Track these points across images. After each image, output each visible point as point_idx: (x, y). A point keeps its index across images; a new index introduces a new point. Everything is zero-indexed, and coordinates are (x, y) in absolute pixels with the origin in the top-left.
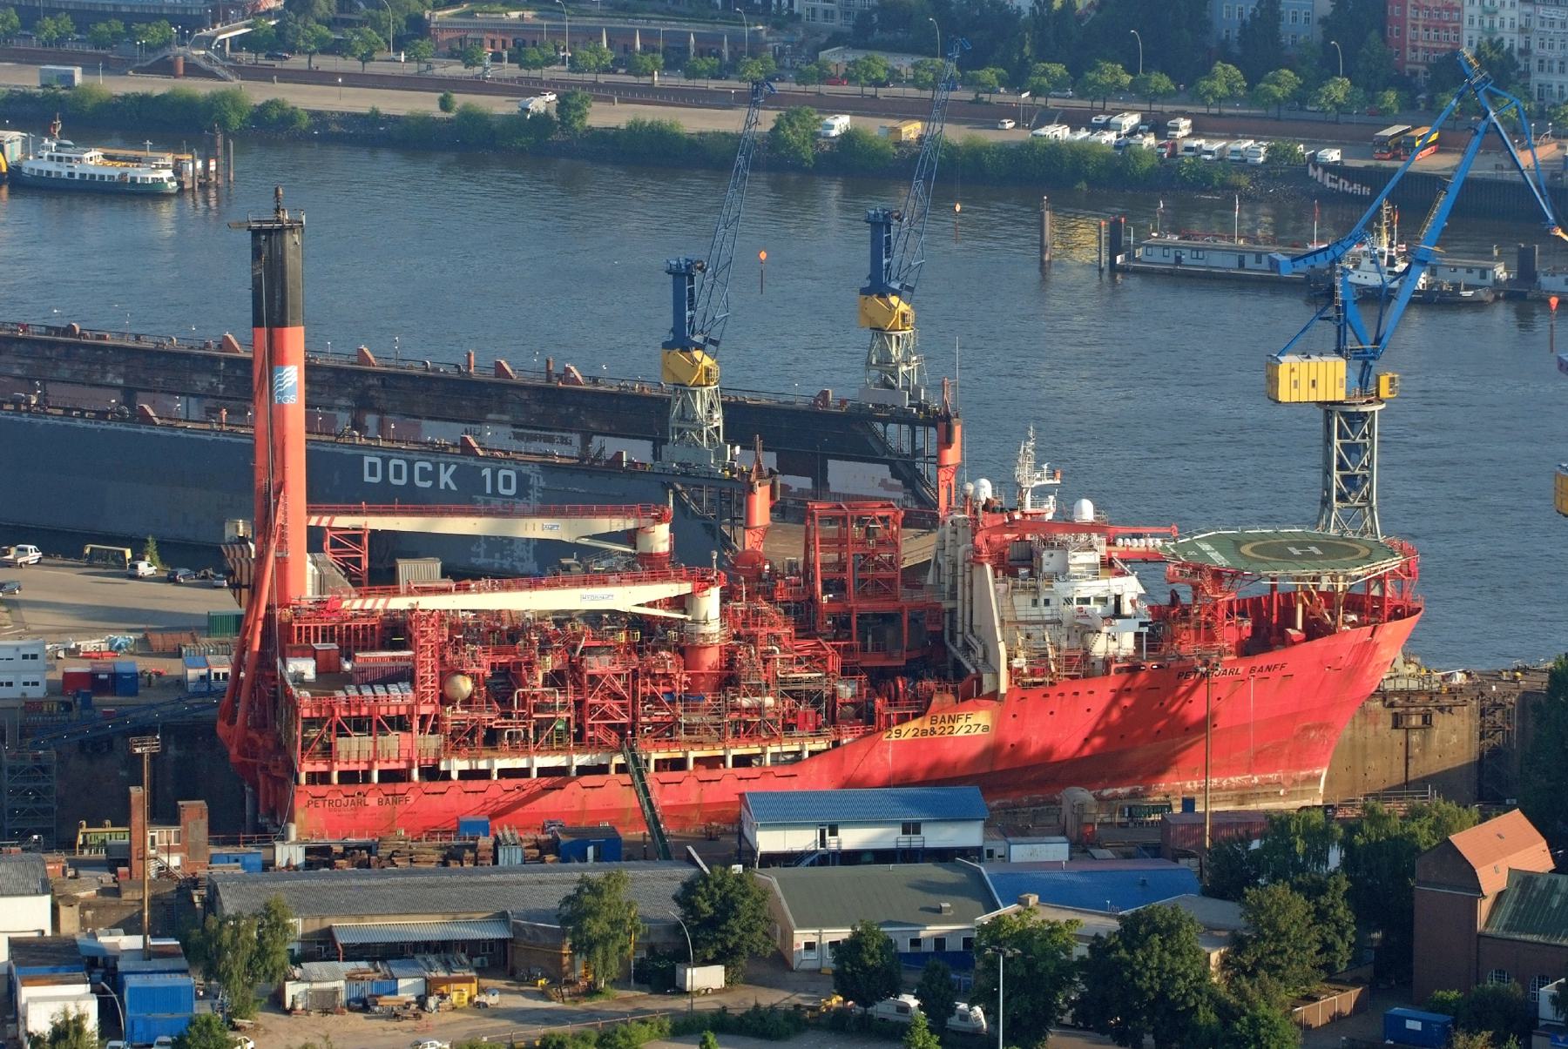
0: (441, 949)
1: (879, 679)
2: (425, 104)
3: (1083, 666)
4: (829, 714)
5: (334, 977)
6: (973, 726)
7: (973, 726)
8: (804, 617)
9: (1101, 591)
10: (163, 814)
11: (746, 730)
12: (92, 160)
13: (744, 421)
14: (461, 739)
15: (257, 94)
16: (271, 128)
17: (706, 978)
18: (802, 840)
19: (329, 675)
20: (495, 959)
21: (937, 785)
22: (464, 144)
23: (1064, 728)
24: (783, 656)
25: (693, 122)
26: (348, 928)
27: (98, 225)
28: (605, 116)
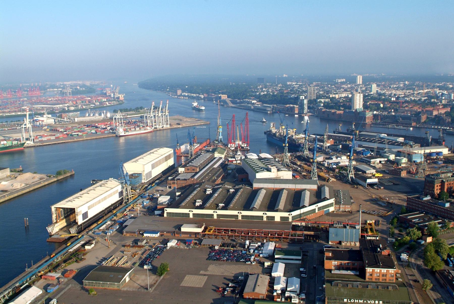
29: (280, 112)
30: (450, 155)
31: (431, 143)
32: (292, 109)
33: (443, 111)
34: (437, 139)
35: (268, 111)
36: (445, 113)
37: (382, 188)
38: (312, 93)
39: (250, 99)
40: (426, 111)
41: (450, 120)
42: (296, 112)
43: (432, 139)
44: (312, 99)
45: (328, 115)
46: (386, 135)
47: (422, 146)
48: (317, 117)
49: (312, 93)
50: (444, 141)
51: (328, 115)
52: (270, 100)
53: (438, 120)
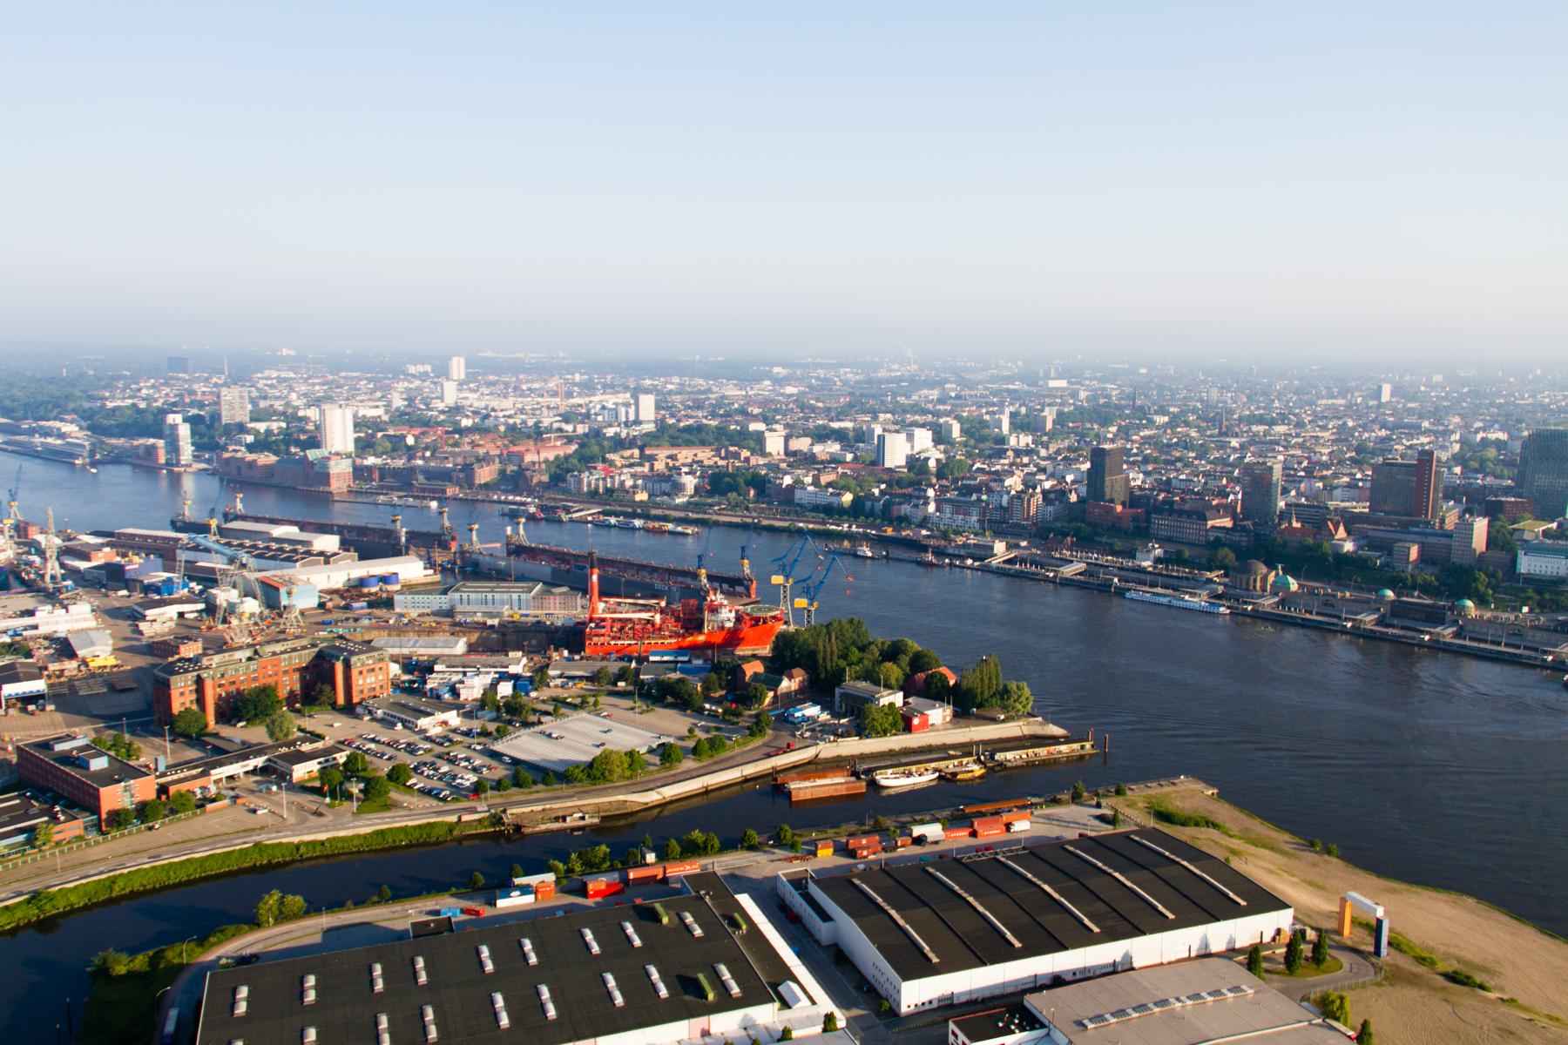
0: (581, 678)
1: (687, 630)
2: (738, 520)
3: (723, 628)
4: (677, 635)
5: (559, 681)
6: (701, 638)
7: (701, 638)
8: (678, 619)
9: (727, 616)
10: (556, 650)
11: (664, 637)
12: (679, 529)
13: (710, 578)
14: (614, 638)
15: (715, 517)
16: (717, 523)
17: (621, 684)
18: (657, 658)
19: (597, 626)
20: (588, 679)
21: (695, 649)
22: (744, 527)
23: (718, 639)
24: (671, 625)
25: (778, 524)
26: (568, 673)
27: (680, 540)
28: (765, 522)
29: (117, 459)
30: (429, 579)
31: (407, 549)
32: (151, 451)
33: (551, 456)
34: (439, 535)
35: (77, 457)
36: (557, 458)
37: (51, 707)
38: (237, 406)
39: (62, 420)
40: (510, 454)
41: (545, 478)
42: (162, 460)
43: (412, 536)
44: (238, 419)
45: (239, 468)
46: (295, 529)
47: (361, 558)
48: (214, 473)
49: (237, 406)
50: (453, 539)
51: (239, 468)
52: (117, 426)
53: (516, 480)
